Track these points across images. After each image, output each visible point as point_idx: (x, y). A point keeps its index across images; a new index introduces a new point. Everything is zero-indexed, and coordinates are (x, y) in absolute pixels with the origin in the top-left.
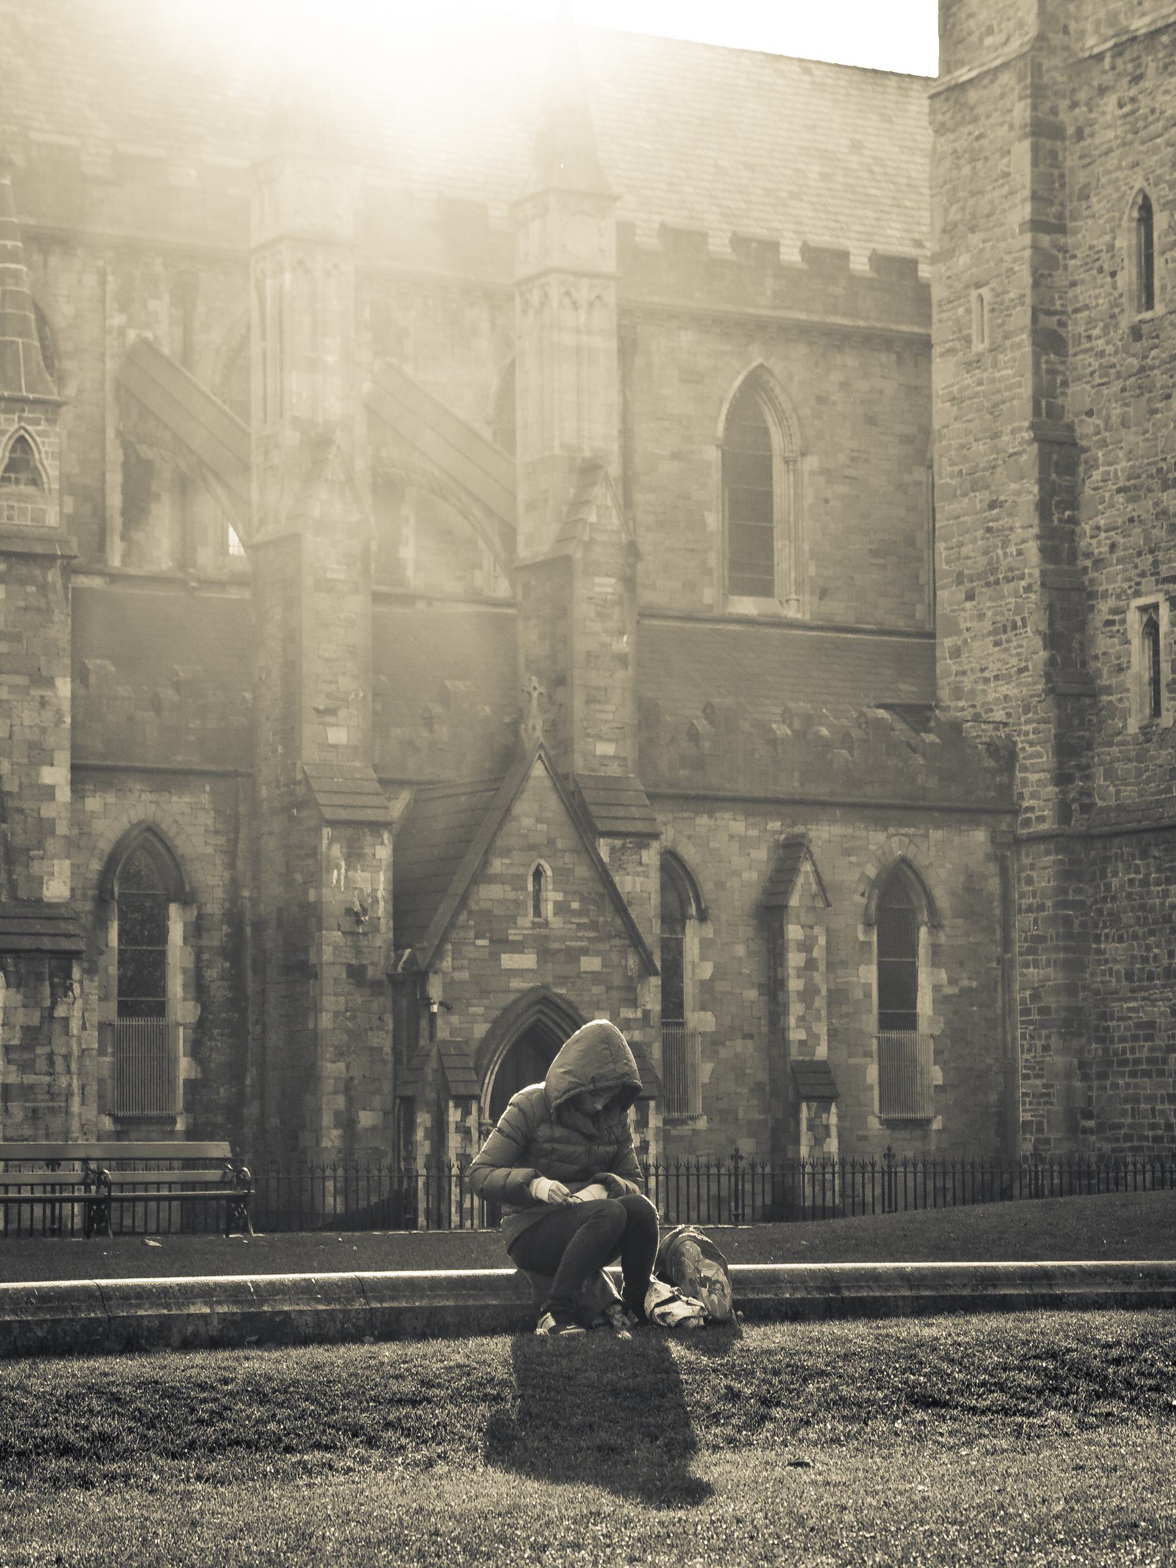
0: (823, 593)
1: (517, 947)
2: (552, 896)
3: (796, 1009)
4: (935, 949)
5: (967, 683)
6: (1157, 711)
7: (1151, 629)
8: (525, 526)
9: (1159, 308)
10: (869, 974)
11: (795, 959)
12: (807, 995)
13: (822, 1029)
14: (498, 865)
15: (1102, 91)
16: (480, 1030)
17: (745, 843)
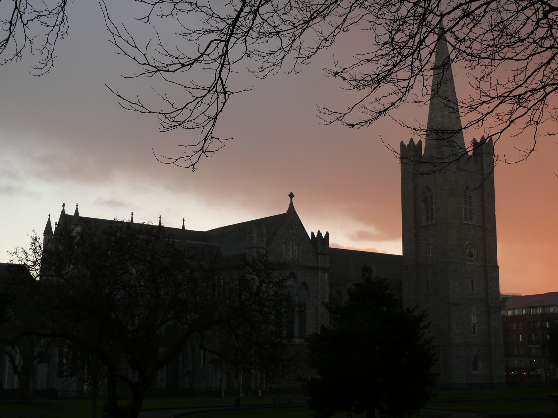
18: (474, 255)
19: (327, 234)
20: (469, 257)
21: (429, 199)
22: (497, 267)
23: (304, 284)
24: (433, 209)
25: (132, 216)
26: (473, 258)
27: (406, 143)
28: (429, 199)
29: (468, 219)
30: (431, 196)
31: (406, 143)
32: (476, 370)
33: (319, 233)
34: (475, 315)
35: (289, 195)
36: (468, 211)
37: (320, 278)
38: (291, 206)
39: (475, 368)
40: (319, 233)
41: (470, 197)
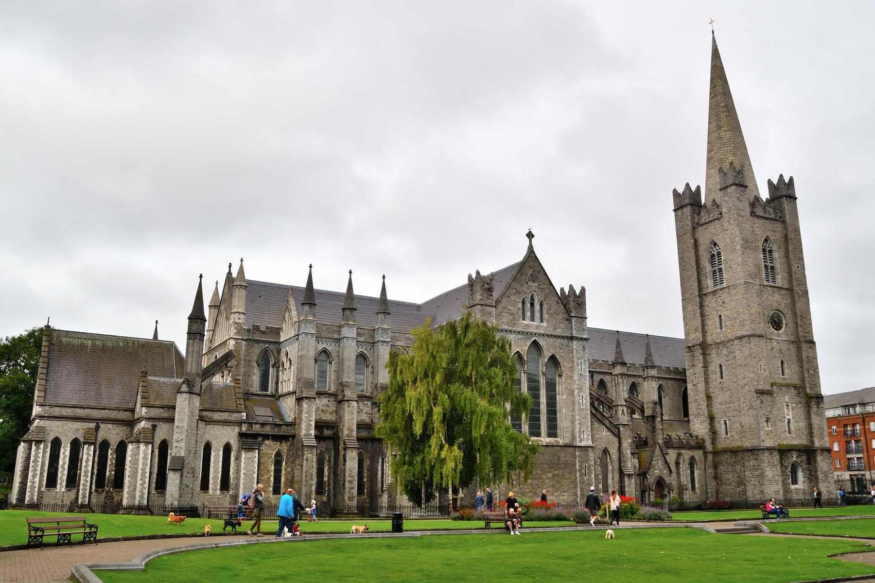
0: (670, 415)
1: (656, 470)
2: (660, 463)
3: (682, 476)
4: (697, 468)
5: (696, 429)
6: (727, 434)
7: (725, 423)
8: (646, 411)
9: (724, 379)
10: (689, 471)
11: (681, 470)
12: (683, 474)
13: (685, 479)
14: (654, 459)
15: (712, 349)
16: (653, 481)
17: (673, 453)
18: (782, 328)
19: (583, 290)
20: (776, 329)
21: (716, 257)
22: (813, 343)
23: (553, 359)
24: (723, 269)
25: (310, 269)
26: (780, 331)
27: (681, 190)
28: (716, 257)
29: (771, 280)
30: (719, 253)
31: (681, 190)
32: (796, 484)
33: (571, 287)
34: (790, 407)
35: (527, 235)
36: (769, 270)
37: (575, 351)
38: (531, 247)
39: (795, 482)
40: (571, 287)
41: (770, 251)
